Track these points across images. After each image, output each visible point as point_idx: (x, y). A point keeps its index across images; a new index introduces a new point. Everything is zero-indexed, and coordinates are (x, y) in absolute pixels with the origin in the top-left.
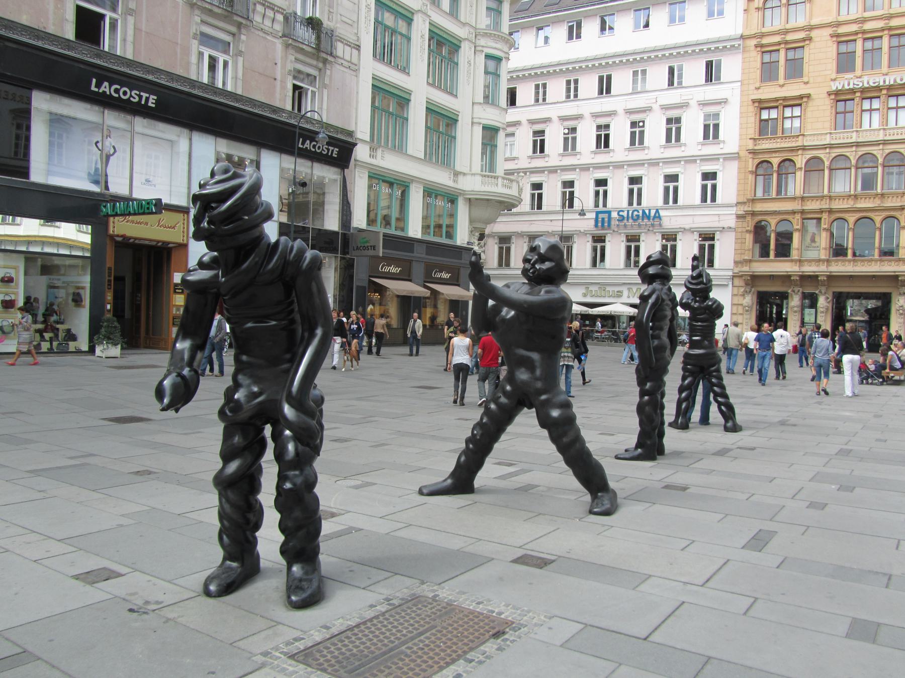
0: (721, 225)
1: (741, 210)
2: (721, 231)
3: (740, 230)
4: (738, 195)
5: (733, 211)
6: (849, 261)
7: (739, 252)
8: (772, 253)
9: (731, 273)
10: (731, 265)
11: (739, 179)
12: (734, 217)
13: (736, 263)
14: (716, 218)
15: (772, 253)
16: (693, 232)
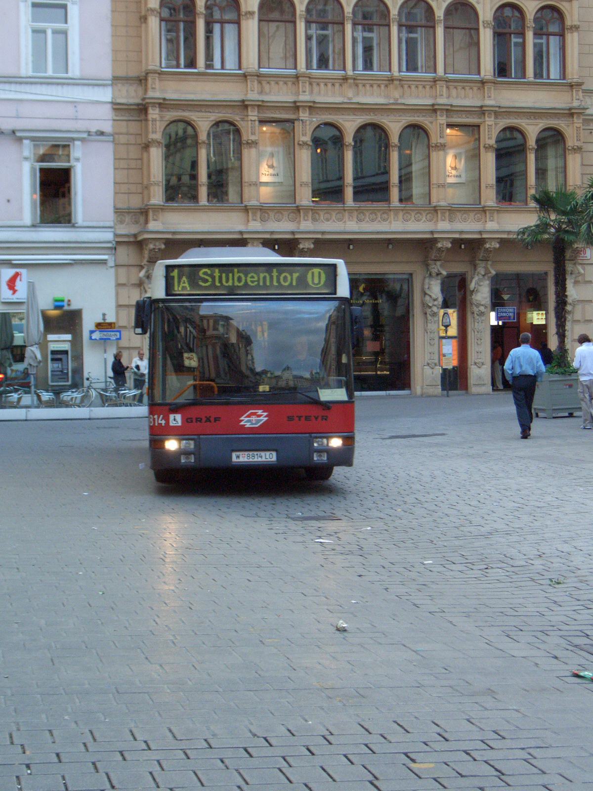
0: (80, 125)
1: (130, 95)
2: (83, 140)
3: (123, 139)
4: (115, 61)
5: (106, 95)
6: (351, 211)
7: (124, 188)
8: (203, 192)
9: (109, 236)
10: (109, 217)
11: (114, 26)
12: (109, 106)
13: (118, 211)
14: (69, 111)
15: (203, 192)
16: (20, 140)
